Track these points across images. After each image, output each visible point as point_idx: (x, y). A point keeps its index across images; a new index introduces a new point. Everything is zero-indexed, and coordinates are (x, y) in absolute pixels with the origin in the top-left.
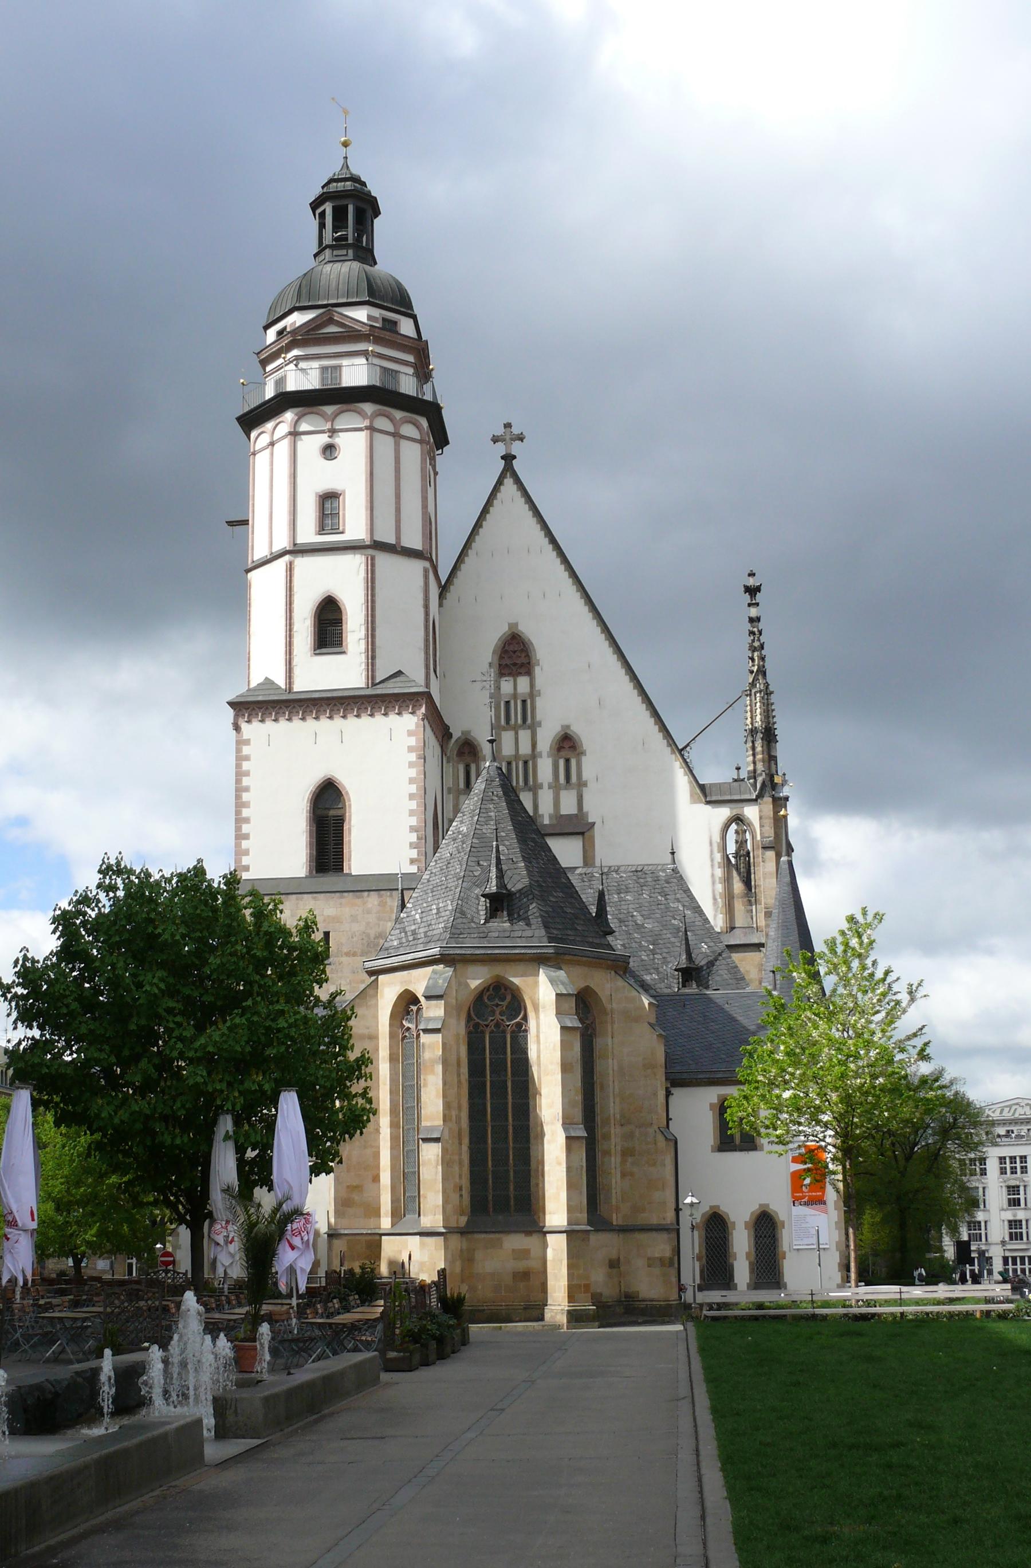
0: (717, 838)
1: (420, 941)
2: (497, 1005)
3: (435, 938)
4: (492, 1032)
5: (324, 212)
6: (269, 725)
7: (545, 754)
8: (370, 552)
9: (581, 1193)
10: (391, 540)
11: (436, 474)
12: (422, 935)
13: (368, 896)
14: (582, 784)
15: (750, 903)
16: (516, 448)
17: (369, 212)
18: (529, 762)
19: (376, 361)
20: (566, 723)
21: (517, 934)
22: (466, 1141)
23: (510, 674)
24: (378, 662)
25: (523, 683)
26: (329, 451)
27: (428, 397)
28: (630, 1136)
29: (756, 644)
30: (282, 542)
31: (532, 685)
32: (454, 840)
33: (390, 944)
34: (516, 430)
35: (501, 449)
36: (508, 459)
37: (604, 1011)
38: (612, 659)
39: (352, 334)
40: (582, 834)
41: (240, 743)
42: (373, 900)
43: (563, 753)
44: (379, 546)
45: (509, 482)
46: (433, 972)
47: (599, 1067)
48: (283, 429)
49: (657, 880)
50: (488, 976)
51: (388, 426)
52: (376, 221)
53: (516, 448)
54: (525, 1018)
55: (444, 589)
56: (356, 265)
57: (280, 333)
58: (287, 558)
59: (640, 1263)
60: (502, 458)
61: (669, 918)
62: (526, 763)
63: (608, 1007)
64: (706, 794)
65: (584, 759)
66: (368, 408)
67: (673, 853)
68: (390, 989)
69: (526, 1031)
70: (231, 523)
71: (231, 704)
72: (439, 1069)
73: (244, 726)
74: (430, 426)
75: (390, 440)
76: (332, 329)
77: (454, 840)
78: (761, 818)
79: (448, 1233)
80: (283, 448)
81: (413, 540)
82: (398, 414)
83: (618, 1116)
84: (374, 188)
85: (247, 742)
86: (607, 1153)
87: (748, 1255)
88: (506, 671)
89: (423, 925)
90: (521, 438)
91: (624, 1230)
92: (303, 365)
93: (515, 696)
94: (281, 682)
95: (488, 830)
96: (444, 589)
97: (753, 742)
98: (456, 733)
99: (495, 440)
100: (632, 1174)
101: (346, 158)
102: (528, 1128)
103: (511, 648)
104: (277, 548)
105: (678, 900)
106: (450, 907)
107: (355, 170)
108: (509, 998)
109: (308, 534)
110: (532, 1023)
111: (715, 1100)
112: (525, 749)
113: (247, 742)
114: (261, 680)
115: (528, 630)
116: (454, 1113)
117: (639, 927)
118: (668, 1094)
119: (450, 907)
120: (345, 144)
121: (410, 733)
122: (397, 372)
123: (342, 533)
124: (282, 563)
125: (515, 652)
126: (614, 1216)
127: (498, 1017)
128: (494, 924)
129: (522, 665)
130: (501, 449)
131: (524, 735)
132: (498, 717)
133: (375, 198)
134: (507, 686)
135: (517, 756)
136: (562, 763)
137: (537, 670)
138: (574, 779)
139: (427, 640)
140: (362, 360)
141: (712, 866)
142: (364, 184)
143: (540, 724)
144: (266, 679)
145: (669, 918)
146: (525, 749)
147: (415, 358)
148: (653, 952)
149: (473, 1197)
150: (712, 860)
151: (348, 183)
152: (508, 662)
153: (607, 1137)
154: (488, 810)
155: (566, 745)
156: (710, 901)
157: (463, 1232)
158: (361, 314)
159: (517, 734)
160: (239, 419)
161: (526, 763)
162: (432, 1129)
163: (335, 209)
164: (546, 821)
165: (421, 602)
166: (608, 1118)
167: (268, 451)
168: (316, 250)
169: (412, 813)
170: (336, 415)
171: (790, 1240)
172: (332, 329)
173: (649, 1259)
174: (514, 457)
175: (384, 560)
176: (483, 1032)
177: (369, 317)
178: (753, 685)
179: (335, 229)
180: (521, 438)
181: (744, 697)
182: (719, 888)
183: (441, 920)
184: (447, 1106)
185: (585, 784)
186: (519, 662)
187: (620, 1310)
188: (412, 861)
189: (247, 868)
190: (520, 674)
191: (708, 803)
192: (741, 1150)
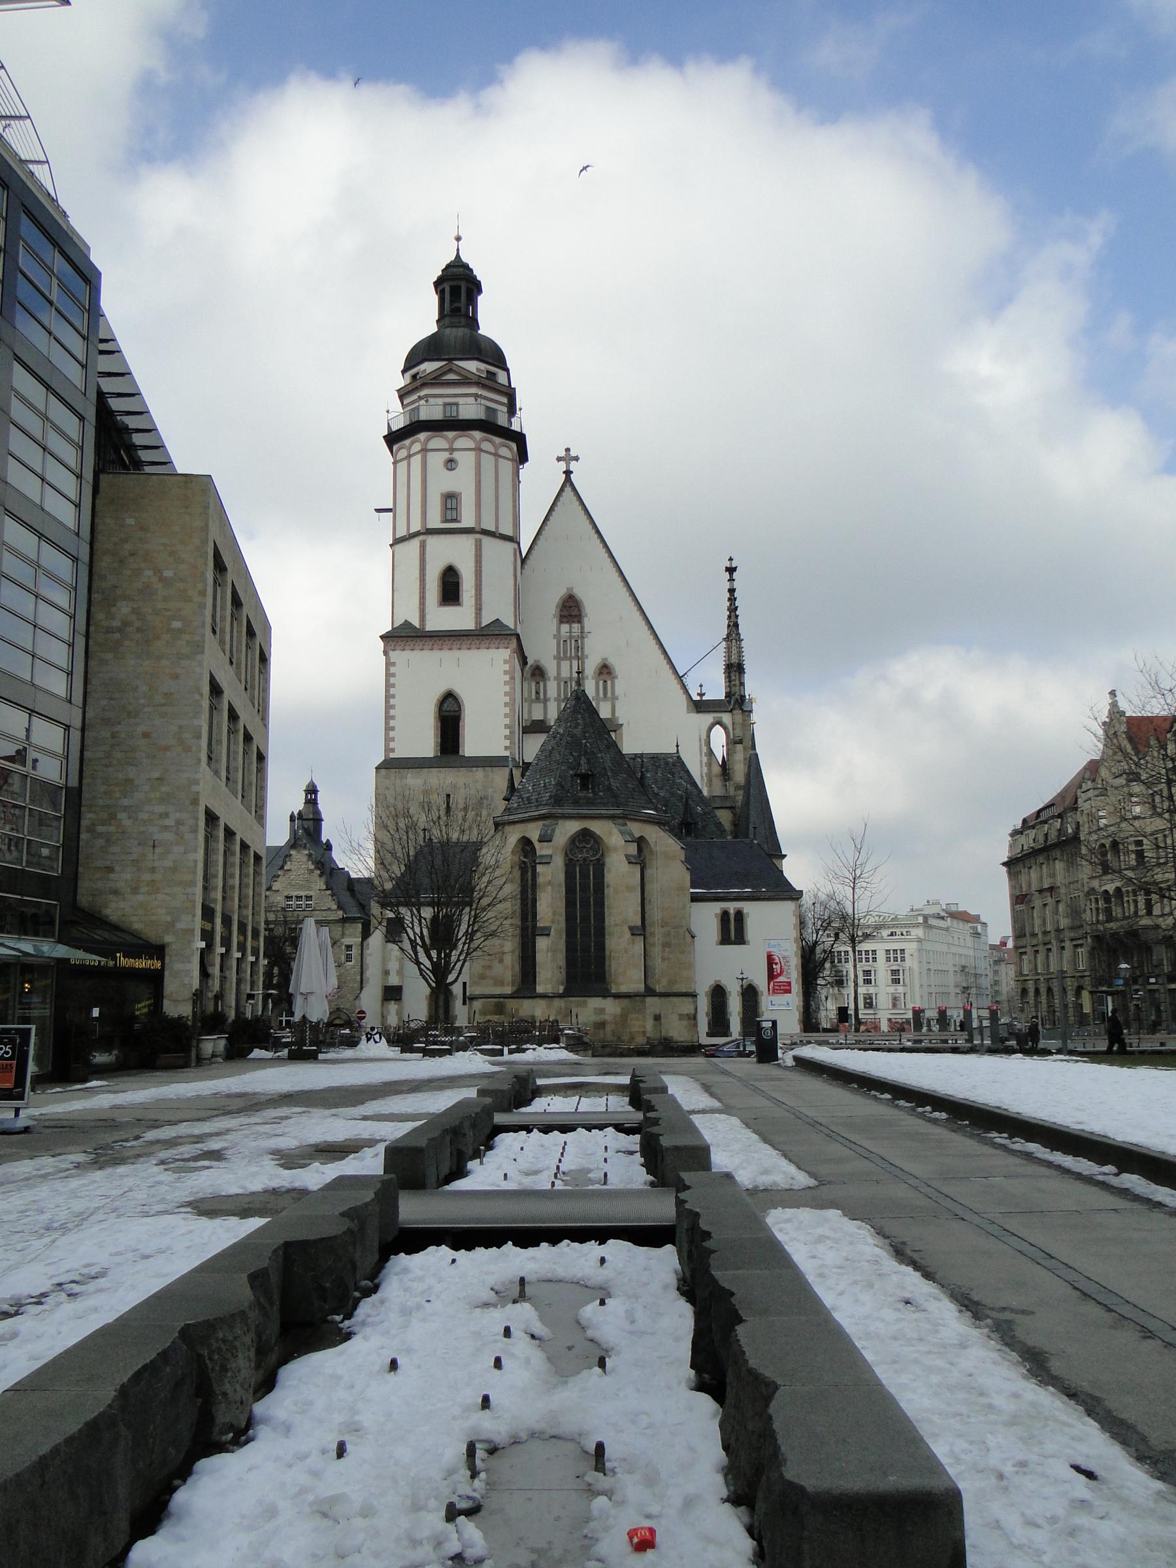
0: (704, 736)
1: (533, 805)
2: (584, 847)
4: (580, 865)
5: (444, 289)
6: (408, 654)
7: (590, 677)
8: (478, 536)
9: (640, 970)
10: (493, 529)
11: (520, 482)
12: (534, 801)
13: (477, 771)
14: (614, 698)
15: (725, 780)
16: (573, 466)
17: (475, 291)
19: (483, 402)
20: (604, 656)
21: (599, 801)
23: (567, 622)
24: (484, 613)
25: (576, 626)
26: (451, 464)
27: (515, 427)
28: (669, 934)
29: (733, 607)
30: (416, 527)
31: (582, 628)
32: (555, 737)
33: (512, 805)
34: (573, 453)
35: (562, 466)
36: (568, 473)
38: (637, 613)
40: (615, 731)
41: (389, 664)
42: (479, 773)
43: (602, 677)
44: (486, 532)
45: (568, 489)
46: (544, 825)
48: (417, 447)
49: (667, 763)
50: (579, 829)
51: (492, 450)
53: (573, 466)
54: (603, 855)
55: (523, 561)
56: (467, 331)
57: (414, 377)
58: (421, 538)
59: (675, 1017)
60: (564, 472)
61: (675, 790)
63: (654, 849)
64: (700, 706)
65: (616, 681)
66: (477, 434)
67: (677, 746)
68: (513, 836)
69: (603, 865)
70: (378, 511)
71: (382, 637)
73: (391, 653)
74: (518, 450)
75: (492, 458)
76: (451, 377)
77: (555, 737)
78: (733, 724)
80: (416, 461)
82: (498, 440)
83: (660, 921)
84: (479, 274)
85: (394, 664)
88: (565, 620)
89: (534, 794)
90: (576, 459)
92: (431, 400)
93: (571, 637)
94: (416, 623)
95: (578, 732)
96: (523, 561)
97: (729, 673)
98: (530, 662)
99: (559, 459)
100: (669, 959)
101: (458, 250)
102: (604, 928)
103: (567, 604)
104: (413, 530)
105: (681, 778)
106: (553, 783)
107: (464, 259)
108: (592, 842)
111: (718, 911)
113: (394, 664)
114: (402, 622)
115: (579, 593)
117: (658, 794)
119: (553, 783)
120: (458, 239)
121: (505, 662)
122: (497, 410)
123: (459, 522)
124: (415, 543)
125: (570, 607)
126: (657, 987)
127: (585, 855)
130: (562, 466)
132: (559, 652)
133: (480, 282)
134: (565, 628)
135: (571, 678)
136: (601, 683)
137: (586, 620)
138: (609, 695)
139: (515, 598)
140: (471, 400)
141: (701, 755)
142: (471, 270)
143: (587, 657)
144: (406, 620)
145: (675, 790)
147: (508, 400)
148: (665, 812)
149: (568, 973)
150: (701, 751)
151: (461, 269)
152: (567, 614)
153: (653, 934)
154: (578, 719)
155: (605, 671)
156: (700, 778)
158: (472, 366)
159: (571, 663)
160: (384, 437)
163: (451, 287)
165: (512, 572)
167: (406, 462)
169: (506, 716)
170: (455, 439)
172: (451, 377)
173: (680, 1015)
174: (572, 472)
175: (487, 541)
176: (575, 865)
177: (478, 370)
178: (729, 635)
179: (452, 302)
180: (576, 459)
181: (724, 643)
182: (705, 770)
183: (547, 791)
185: (617, 699)
186: (573, 614)
187: (660, 1048)
188: (506, 748)
189: (393, 750)
191: (698, 712)
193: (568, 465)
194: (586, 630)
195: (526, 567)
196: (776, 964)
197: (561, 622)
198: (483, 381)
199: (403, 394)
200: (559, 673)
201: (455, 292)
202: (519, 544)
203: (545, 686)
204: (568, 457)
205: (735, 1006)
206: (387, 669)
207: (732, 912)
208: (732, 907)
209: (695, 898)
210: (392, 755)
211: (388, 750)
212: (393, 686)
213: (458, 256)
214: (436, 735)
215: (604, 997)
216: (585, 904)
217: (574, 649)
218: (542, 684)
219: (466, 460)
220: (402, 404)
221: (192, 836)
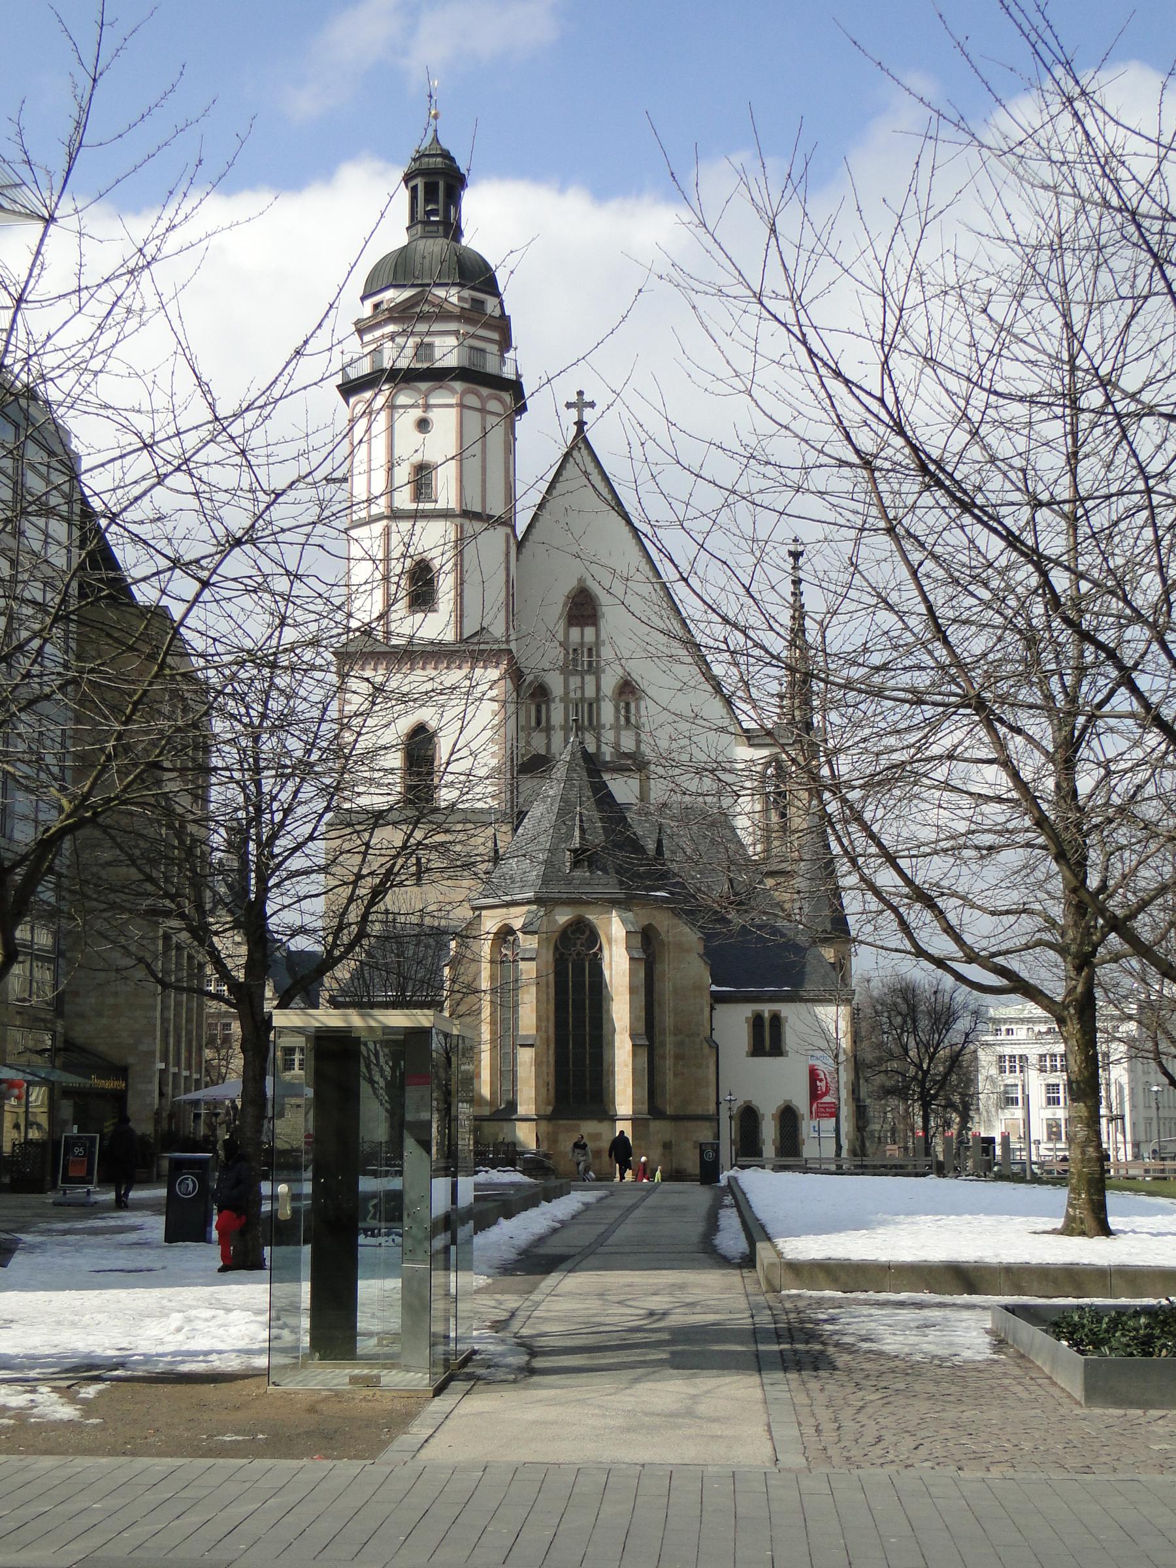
3: (530, 883)
8: (458, 521)
10: (478, 509)
11: (515, 439)
16: (588, 415)
18: (593, 704)
22: (552, 1046)
23: (577, 625)
25: (589, 632)
26: (423, 425)
29: (798, 604)
31: (598, 635)
34: (587, 398)
35: (573, 414)
36: (580, 424)
37: (662, 943)
39: (443, 314)
43: (623, 697)
44: (466, 514)
47: (657, 986)
48: (380, 401)
51: (477, 403)
53: (588, 415)
54: (601, 949)
55: (520, 545)
57: (376, 306)
58: (385, 522)
62: (590, 705)
63: (666, 940)
66: (458, 386)
72: (533, 989)
75: (478, 415)
79: (539, 1118)
80: (381, 420)
81: (496, 508)
82: (485, 391)
86: (663, 1057)
87: (774, 1141)
90: (592, 405)
91: (676, 1118)
93: (582, 644)
96: (520, 545)
99: (569, 405)
100: (683, 1074)
107: (446, 144)
108: (588, 933)
109: (404, 500)
110: (606, 953)
112: (590, 692)
116: (544, 1024)
118: (712, 1009)
128: (577, 873)
129: (589, 617)
130: (573, 414)
131: (590, 680)
134: (575, 633)
135: (583, 699)
142: (452, 160)
146: (590, 692)
151: (439, 159)
153: (663, 1044)
157: (549, 1118)
159: (583, 678)
160: (338, 387)
161: (590, 705)
162: (527, 1037)
163: (426, 185)
164: (608, 759)
166: (664, 1029)
168: (407, 224)
171: (807, 1127)
177: (460, 299)
179: (427, 201)
180: (592, 405)
184: (539, 1018)
190: (588, 625)
191: (751, 746)
192: (770, 1056)
194: (603, 636)
195: (524, 550)
196: (821, 1080)
198: (467, 314)
200: (567, 693)
201: (431, 192)
202: (513, 528)
203: (548, 710)
204: (581, 403)
205: (769, 1131)
207: (766, 1015)
208: (766, 1009)
209: (718, 999)
213: (436, 140)
215: (601, 1120)
216: (579, 1007)
218: (544, 707)
219: (445, 419)
220: (362, 339)
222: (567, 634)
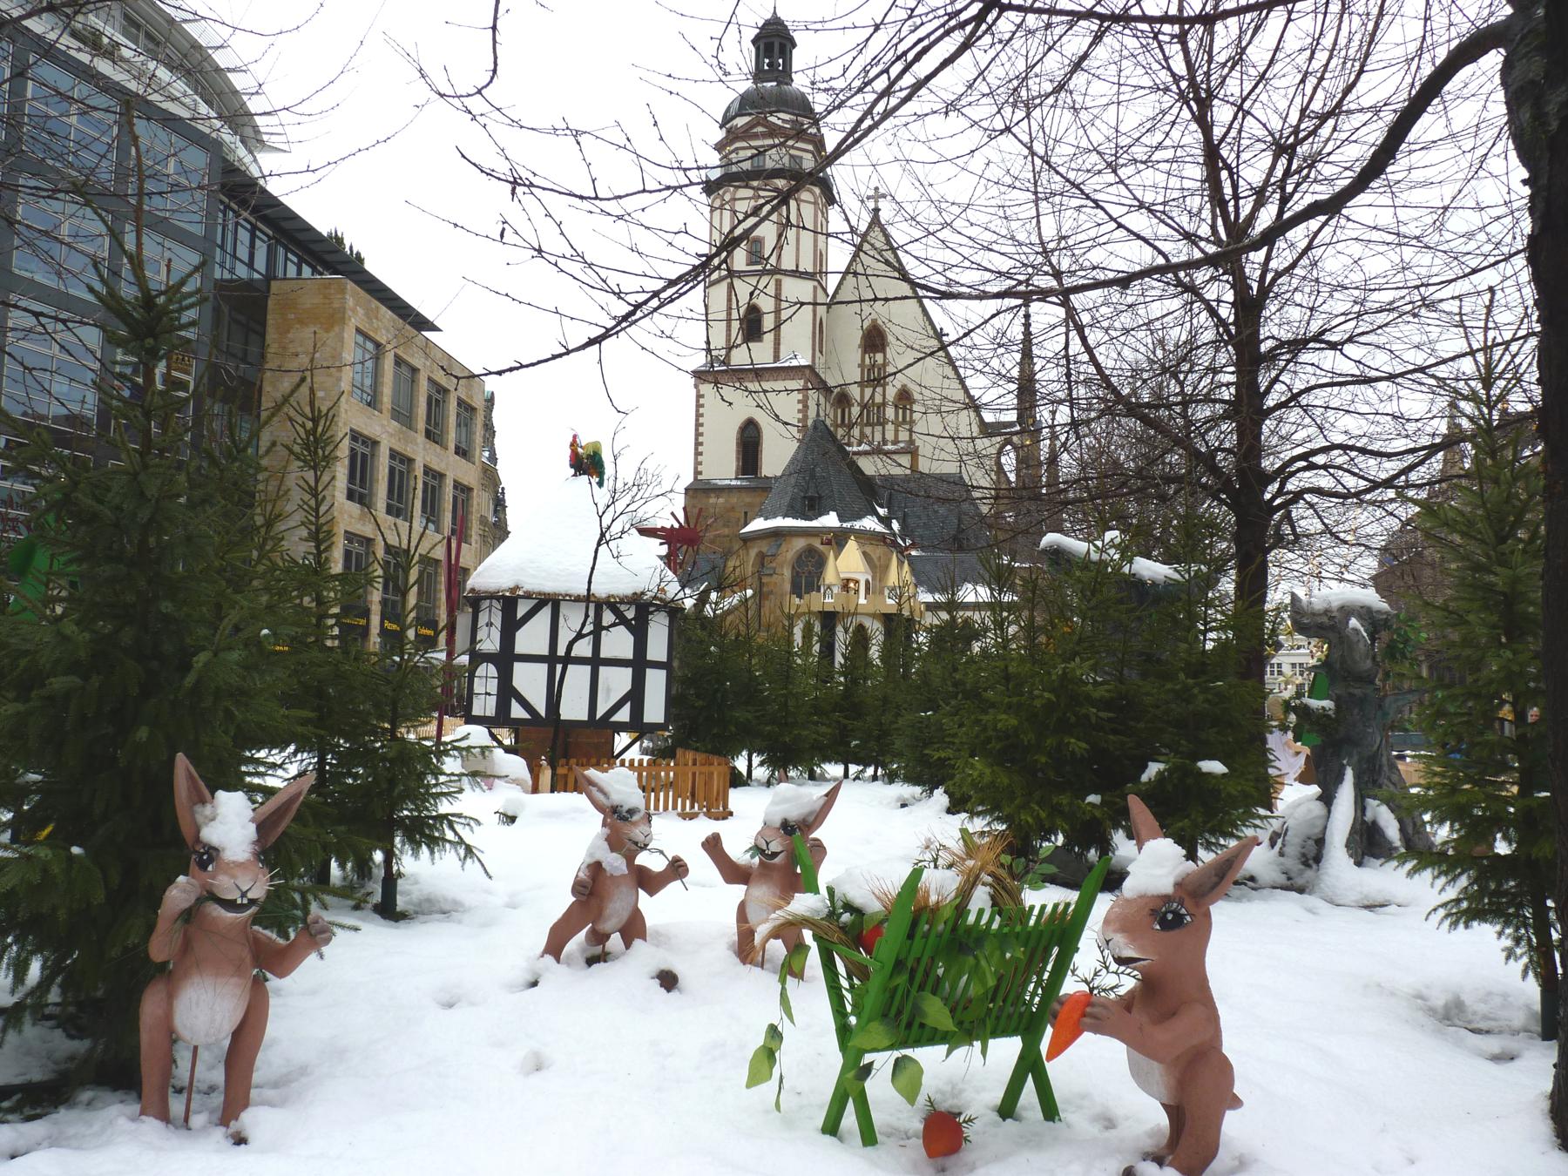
8: (778, 277)
17: (789, 46)
25: (879, 357)
34: (881, 191)
41: (699, 396)
48: (727, 197)
52: (794, 51)
57: (728, 131)
73: (701, 387)
85: (702, 396)
107: (781, 14)
113: (702, 396)
139: (814, 333)
161: (879, 408)
172: (760, 129)
189: (701, 473)
193: (876, 202)
197: (865, 352)
199: (719, 147)
206: (698, 401)
210: (700, 477)
211: (697, 473)
212: (702, 415)
214: (738, 459)
217: (875, 378)
221: (297, 475)
222: (863, 360)
